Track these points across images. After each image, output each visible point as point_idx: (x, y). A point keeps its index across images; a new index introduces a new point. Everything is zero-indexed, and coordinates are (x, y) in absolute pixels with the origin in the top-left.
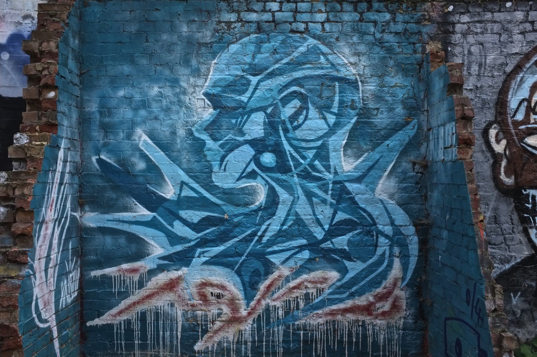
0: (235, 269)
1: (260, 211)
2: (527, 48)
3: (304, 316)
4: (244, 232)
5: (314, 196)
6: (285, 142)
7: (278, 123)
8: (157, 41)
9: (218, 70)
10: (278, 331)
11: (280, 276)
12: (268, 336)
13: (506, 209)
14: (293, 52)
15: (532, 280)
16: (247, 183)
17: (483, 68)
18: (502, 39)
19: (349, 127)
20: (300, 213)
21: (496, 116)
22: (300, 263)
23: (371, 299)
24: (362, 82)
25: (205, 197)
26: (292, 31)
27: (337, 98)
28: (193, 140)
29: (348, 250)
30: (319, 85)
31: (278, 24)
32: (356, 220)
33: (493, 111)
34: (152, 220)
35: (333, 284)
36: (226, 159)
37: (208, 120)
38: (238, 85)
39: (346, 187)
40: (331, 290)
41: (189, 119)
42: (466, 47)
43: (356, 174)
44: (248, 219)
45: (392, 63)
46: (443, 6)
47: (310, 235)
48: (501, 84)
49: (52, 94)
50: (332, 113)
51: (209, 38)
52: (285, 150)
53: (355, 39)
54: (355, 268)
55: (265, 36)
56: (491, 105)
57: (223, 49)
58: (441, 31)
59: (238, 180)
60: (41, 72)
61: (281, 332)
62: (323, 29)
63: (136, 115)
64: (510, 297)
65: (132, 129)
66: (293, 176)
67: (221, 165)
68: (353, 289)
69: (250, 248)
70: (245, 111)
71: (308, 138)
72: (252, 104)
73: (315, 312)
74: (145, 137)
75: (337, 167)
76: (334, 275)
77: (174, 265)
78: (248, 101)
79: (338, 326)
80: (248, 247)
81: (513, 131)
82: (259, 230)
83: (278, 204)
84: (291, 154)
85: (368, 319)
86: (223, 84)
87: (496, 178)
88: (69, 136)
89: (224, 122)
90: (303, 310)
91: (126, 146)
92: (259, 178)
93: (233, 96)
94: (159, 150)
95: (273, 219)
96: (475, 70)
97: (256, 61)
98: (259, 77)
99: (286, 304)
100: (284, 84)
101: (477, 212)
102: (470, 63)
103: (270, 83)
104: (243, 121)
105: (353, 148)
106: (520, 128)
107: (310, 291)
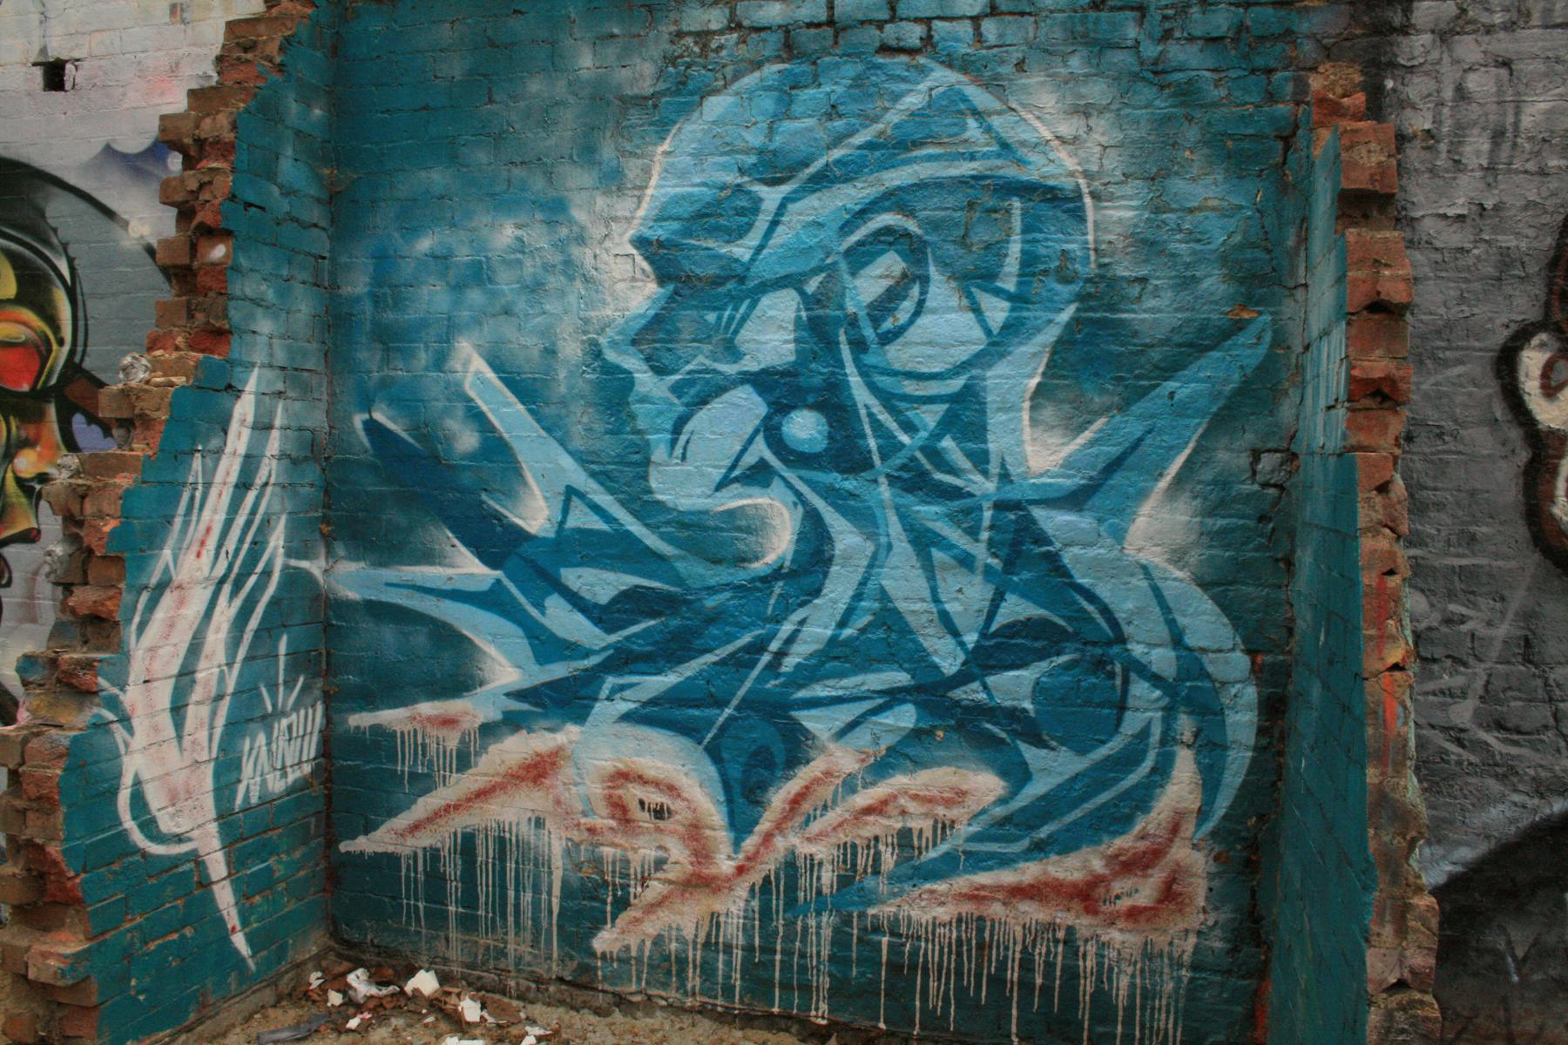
0: (706, 741)
1: (777, 579)
3: (895, 895)
4: (730, 638)
5: (935, 544)
6: (855, 380)
7: (837, 322)
8: (514, 98)
9: (672, 170)
10: (819, 927)
11: (828, 774)
12: (789, 937)
14: (886, 109)
16: (740, 496)
17: (1506, 146)
19: (1050, 335)
20: (892, 592)
21: (1547, 306)
22: (887, 741)
23: (1098, 865)
24: (1095, 196)
25: (628, 534)
26: (885, 49)
27: (1015, 249)
28: (602, 373)
29: (1032, 714)
30: (962, 209)
31: (844, 29)
32: (1062, 623)
33: (1538, 289)
34: (491, 591)
35: (983, 811)
36: (689, 427)
37: (642, 316)
38: (721, 214)
39: (1034, 522)
40: (974, 829)
41: (593, 314)
42: (1450, 75)
43: (1069, 483)
44: (743, 601)
45: (1192, 133)
47: (919, 660)
49: (219, 252)
50: (998, 292)
51: (649, 82)
52: (855, 405)
53: (1075, 63)
54: (1052, 767)
55: (806, 67)
56: (1533, 269)
57: (686, 110)
58: (1365, 26)
59: (720, 486)
61: (827, 933)
62: (979, 37)
63: (457, 304)
65: (448, 341)
66: (875, 481)
67: (674, 442)
68: (1044, 832)
69: (748, 684)
70: (740, 286)
71: (924, 370)
72: (767, 268)
73: (928, 886)
74: (479, 364)
75: (1008, 459)
76: (985, 784)
77: (545, 716)
78: (753, 260)
79: (992, 935)
80: (742, 682)
82: (772, 636)
83: (829, 561)
84: (871, 415)
85: (1083, 924)
86: (686, 210)
88: (281, 357)
89: (686, 319)
90: (893, 878)
91: (433, 385)
92: (777, 483)
93: (711, 244)
94: (512, 398)
95: (816, 606)
96: (1478, 153)
97: (778, 140)
98: (785, 189)
99: (845, 855)
100: (858, 208)
101: (1381, 637)
102: (1460, 130)
103: (816, 203)
104: (738, 316)
105: (1062, 402)
107: (915, 824)
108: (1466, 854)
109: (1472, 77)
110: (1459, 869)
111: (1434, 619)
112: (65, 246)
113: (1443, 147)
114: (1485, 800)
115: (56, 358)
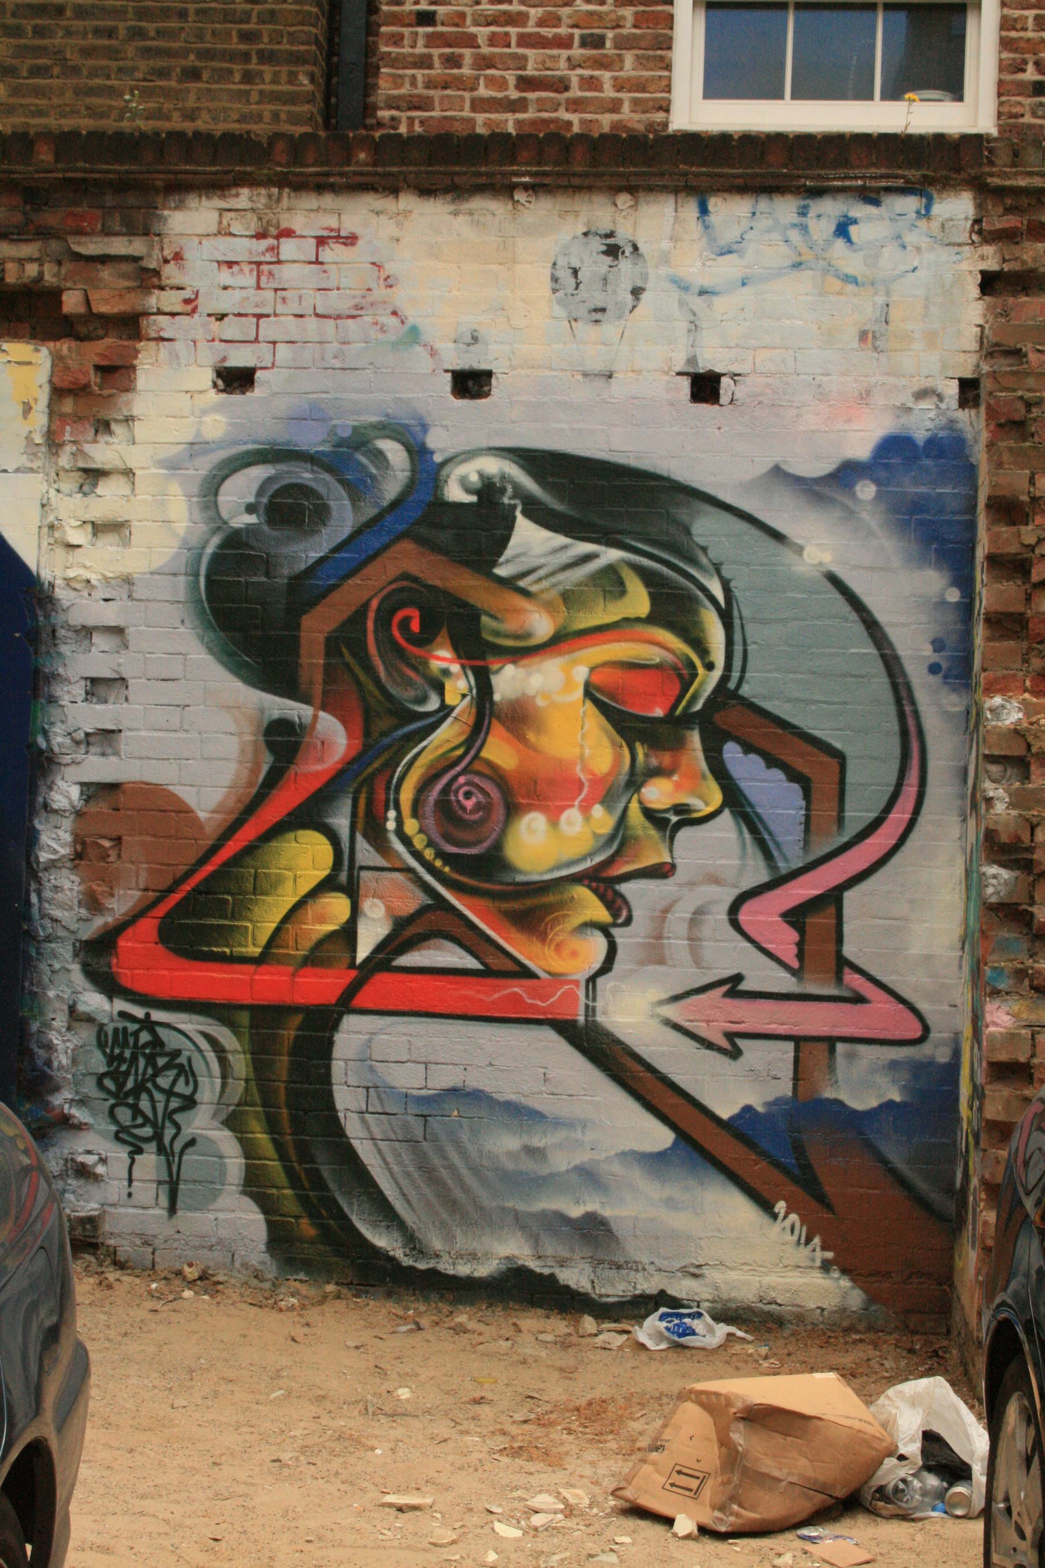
60: (1032, 548)
112: (717, 568)
115: (702, 683)
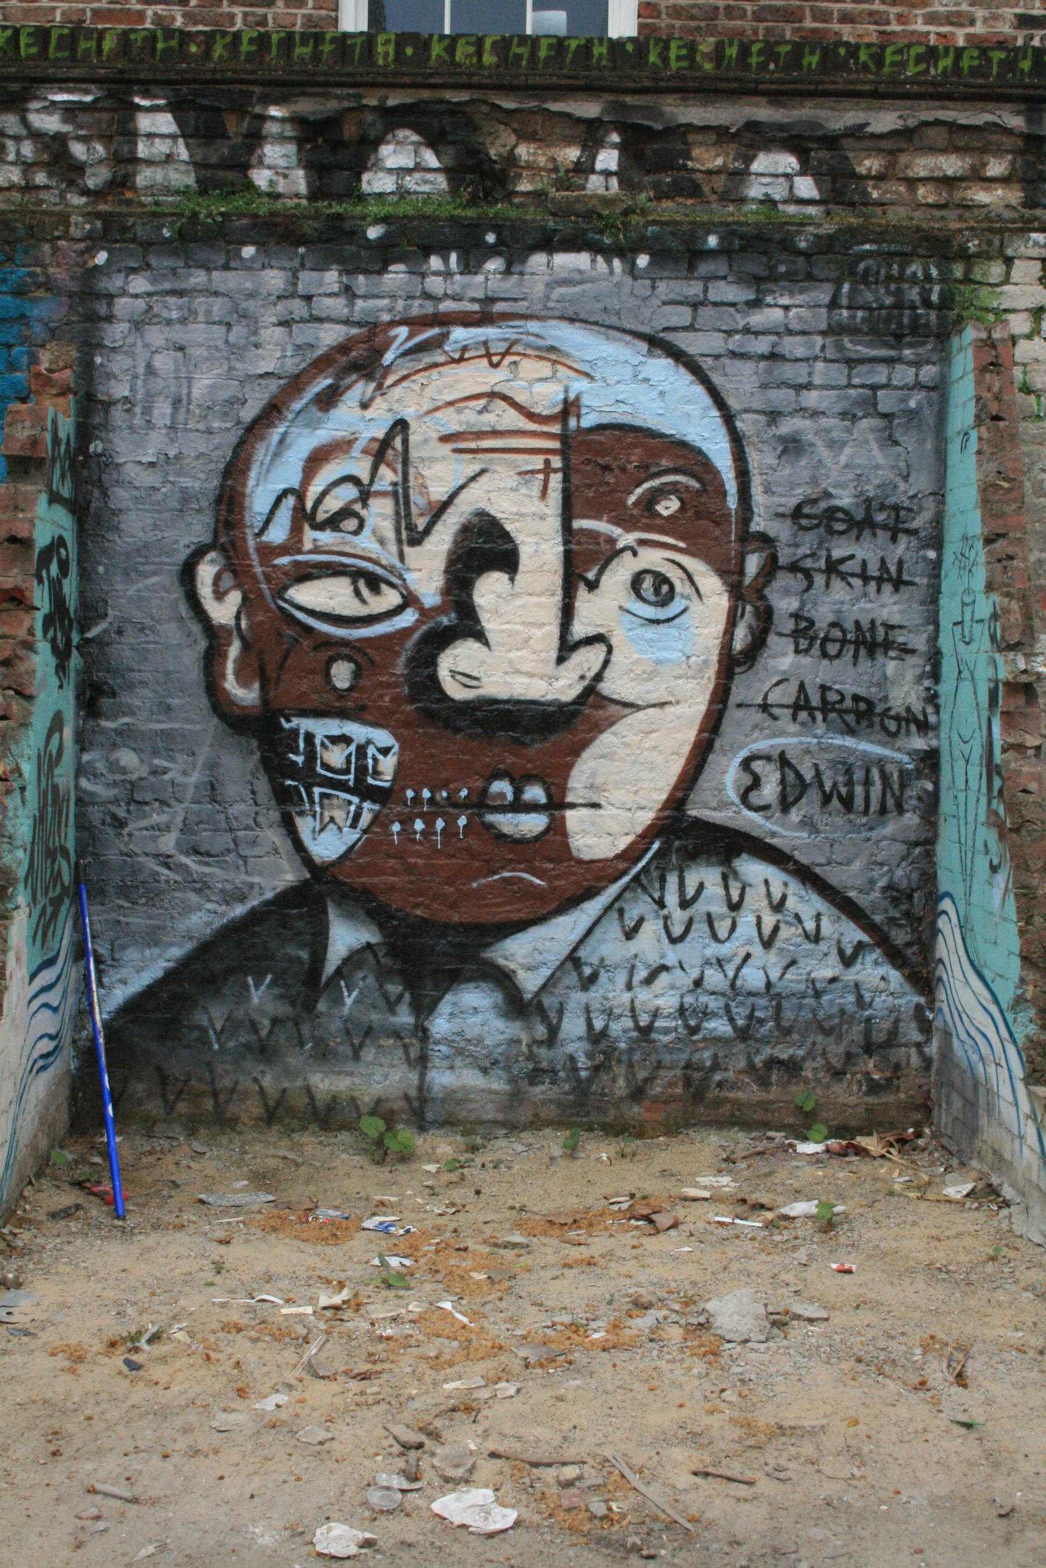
2: (297, 360)
13: (240, 768)
15: (302, 945)
17: (183, 410)
18: (232, 338)
21: (216, 532)
33: (208, 518)
42: (142, 356)
46: (82, 253)
48: (230, 453)
56: (204, 503)
58: (79, 314)
64: (246, 987)
81: (258, 570)
87: (212, 686)
96: (163, 416)
102: (150, 396)
106: (277, 562)
108: (176, 952)
109: (157, 357)
110: (172, 964)
111: (144, 771)
113: (138, 410)
114: (188, 909)
